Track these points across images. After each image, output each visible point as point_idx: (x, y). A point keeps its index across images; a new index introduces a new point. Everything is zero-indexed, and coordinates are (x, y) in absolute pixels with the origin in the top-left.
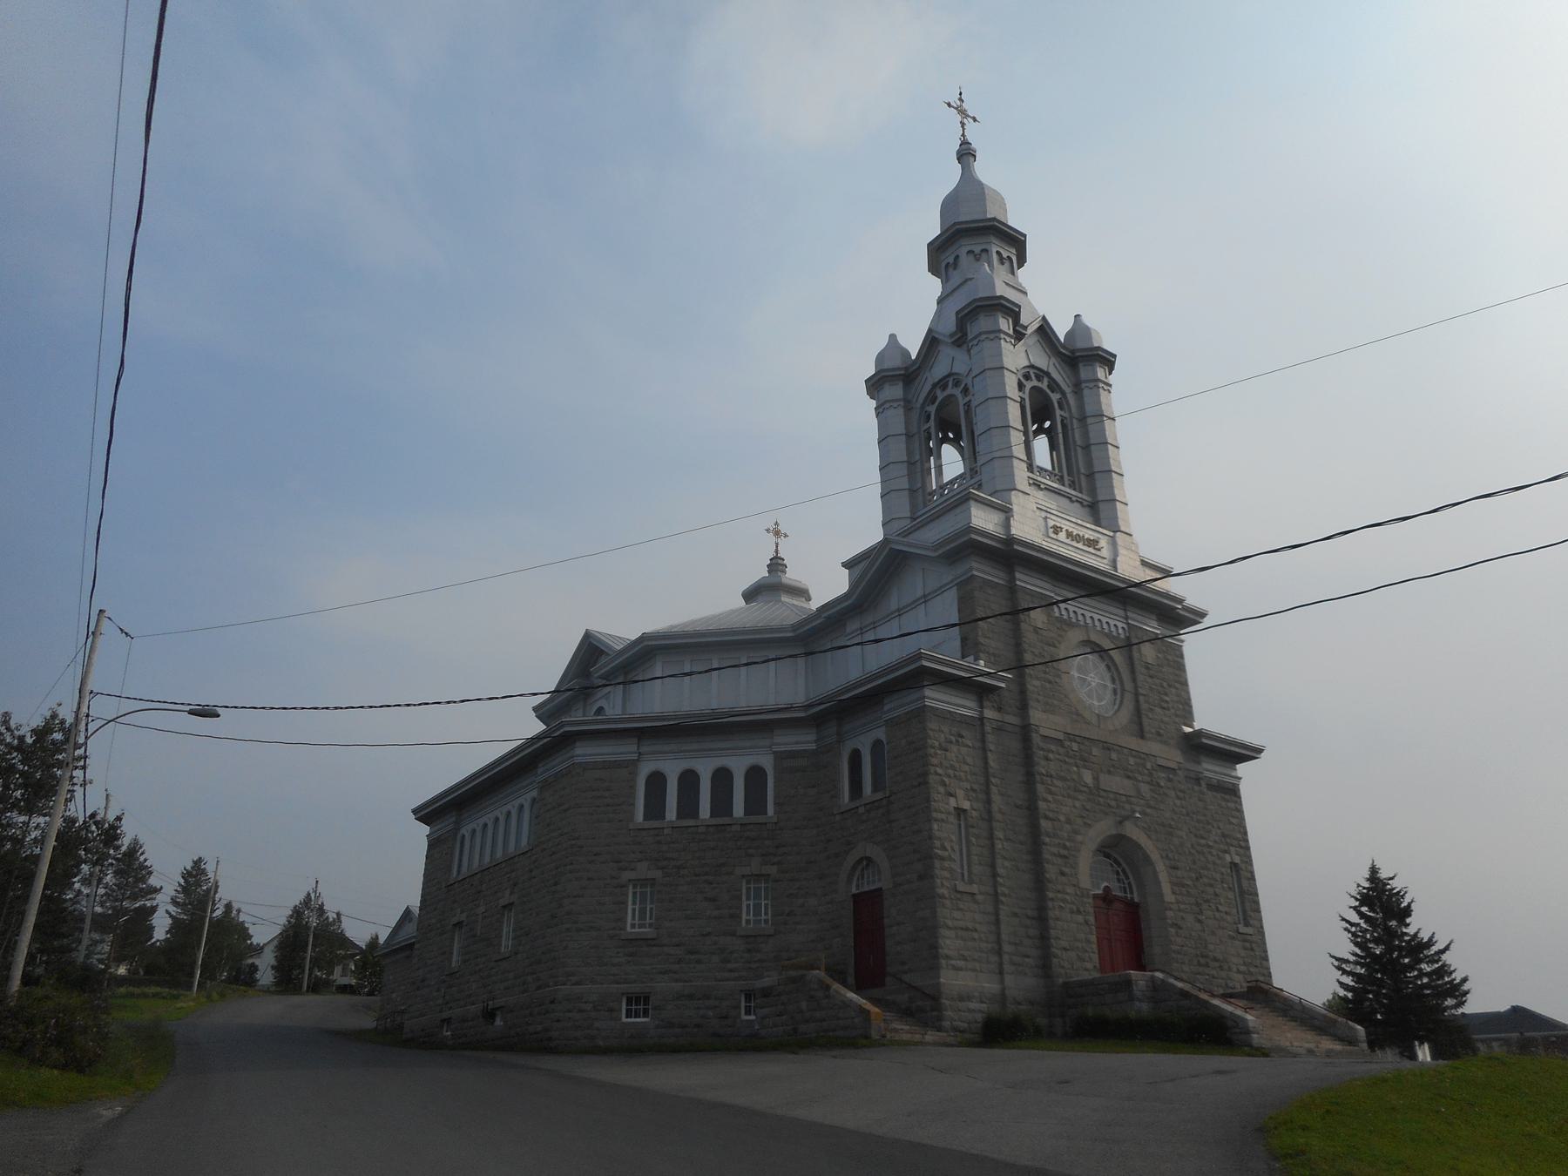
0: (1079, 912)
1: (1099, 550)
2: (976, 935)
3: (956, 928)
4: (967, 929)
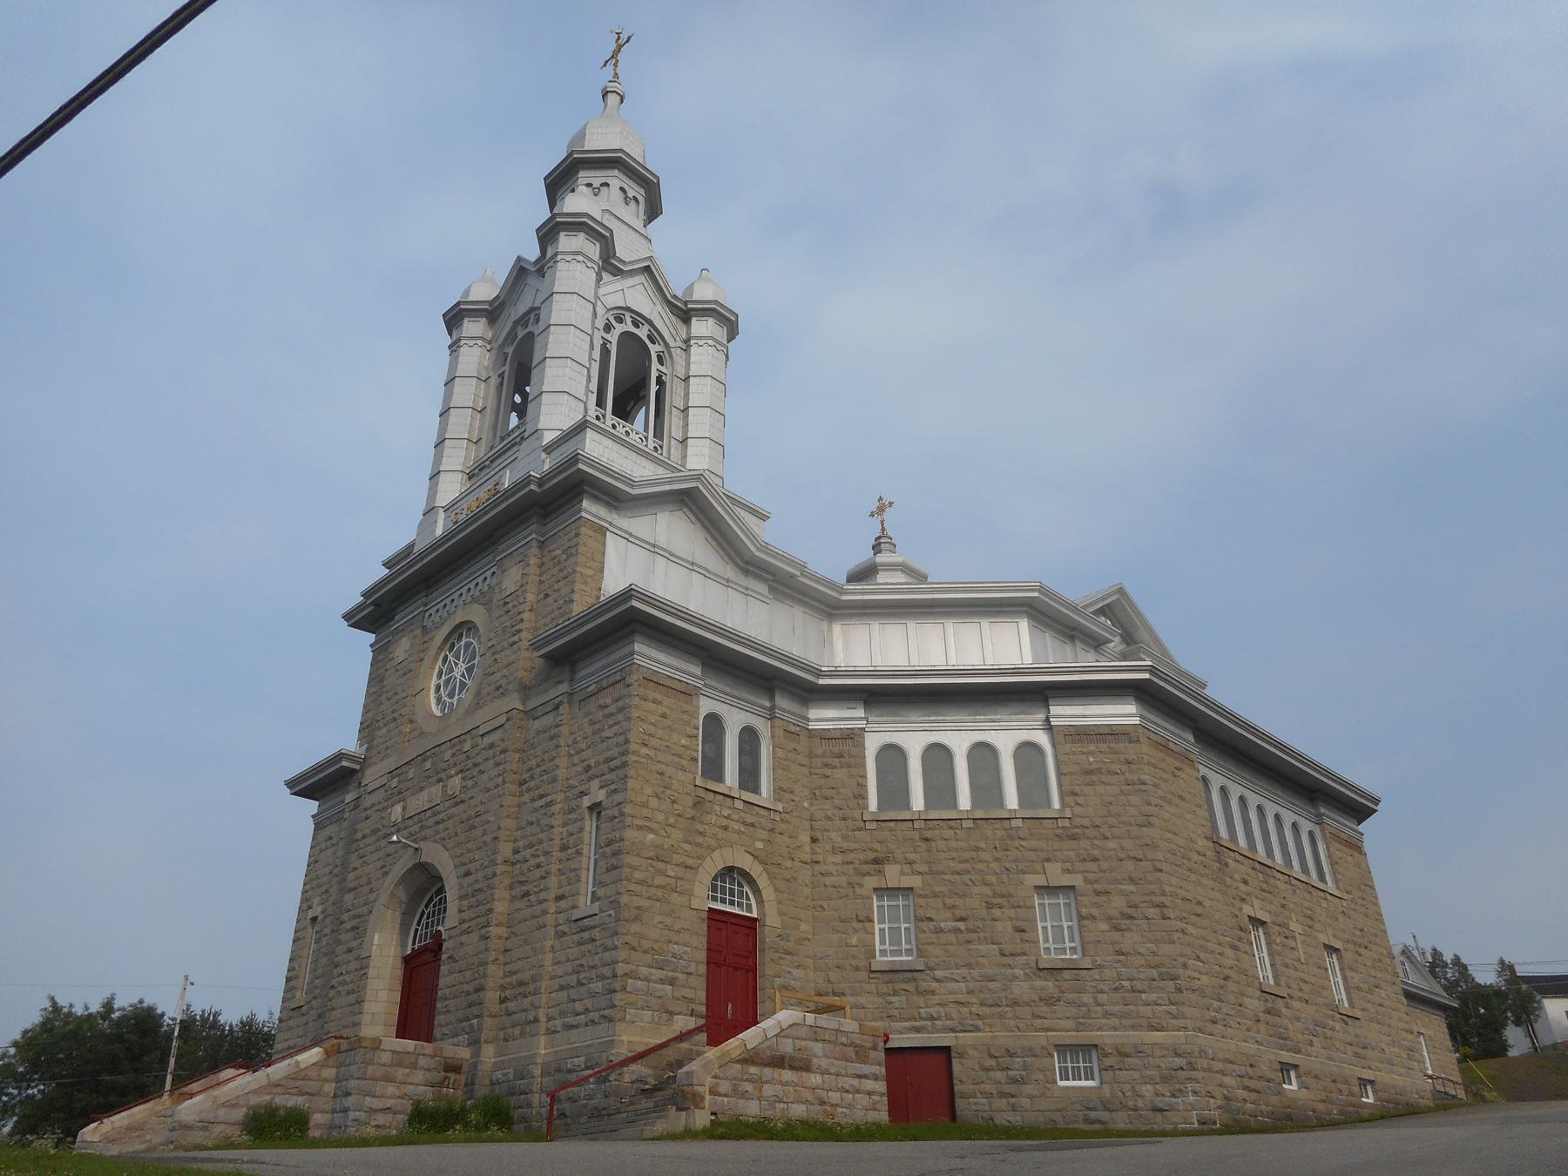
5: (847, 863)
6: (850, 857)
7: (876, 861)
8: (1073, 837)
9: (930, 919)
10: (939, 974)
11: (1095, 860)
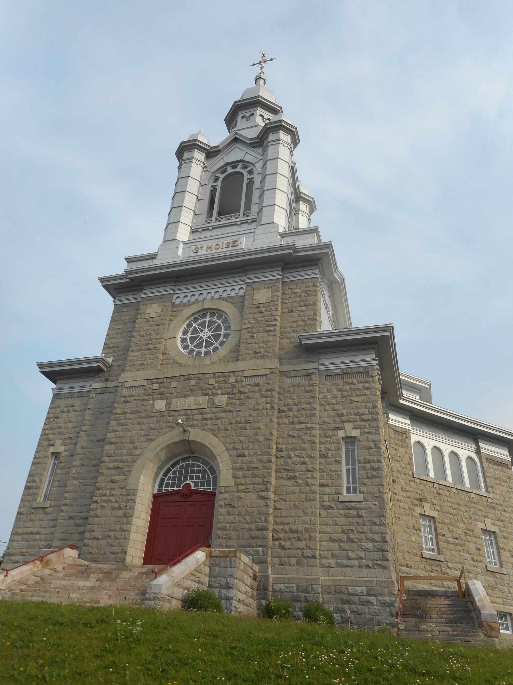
0: (120, 508)
1: (237, 246)
2: (37, 537)
3: (23, 534)
4: (32, 533)
5: (408, 497)
6: (409, 495)
7: (420, 500)
8: (494, 508)
9: (444, 535)
10: (450, 565)
11: (502, 521)
